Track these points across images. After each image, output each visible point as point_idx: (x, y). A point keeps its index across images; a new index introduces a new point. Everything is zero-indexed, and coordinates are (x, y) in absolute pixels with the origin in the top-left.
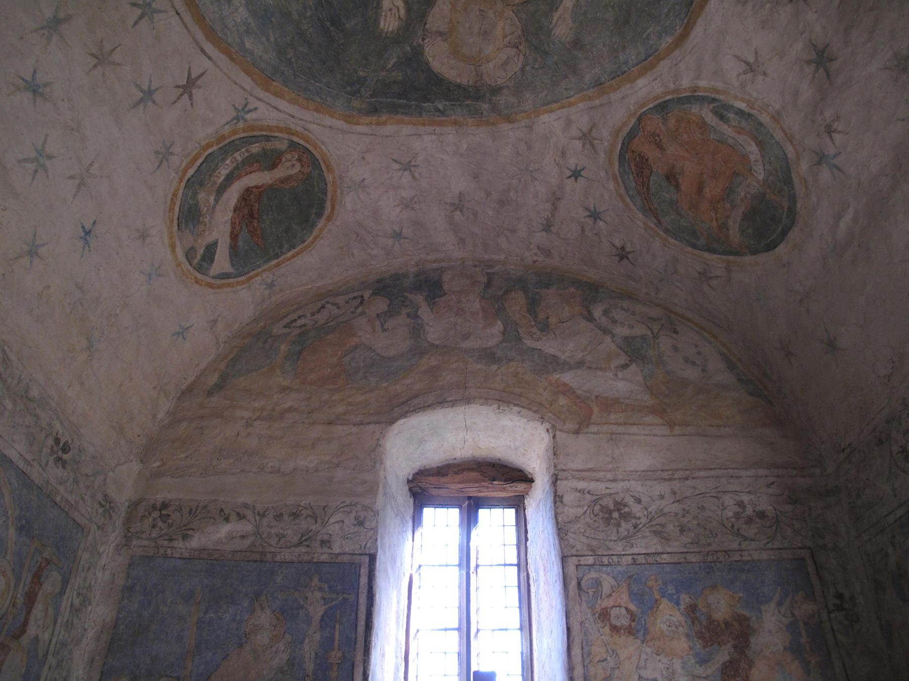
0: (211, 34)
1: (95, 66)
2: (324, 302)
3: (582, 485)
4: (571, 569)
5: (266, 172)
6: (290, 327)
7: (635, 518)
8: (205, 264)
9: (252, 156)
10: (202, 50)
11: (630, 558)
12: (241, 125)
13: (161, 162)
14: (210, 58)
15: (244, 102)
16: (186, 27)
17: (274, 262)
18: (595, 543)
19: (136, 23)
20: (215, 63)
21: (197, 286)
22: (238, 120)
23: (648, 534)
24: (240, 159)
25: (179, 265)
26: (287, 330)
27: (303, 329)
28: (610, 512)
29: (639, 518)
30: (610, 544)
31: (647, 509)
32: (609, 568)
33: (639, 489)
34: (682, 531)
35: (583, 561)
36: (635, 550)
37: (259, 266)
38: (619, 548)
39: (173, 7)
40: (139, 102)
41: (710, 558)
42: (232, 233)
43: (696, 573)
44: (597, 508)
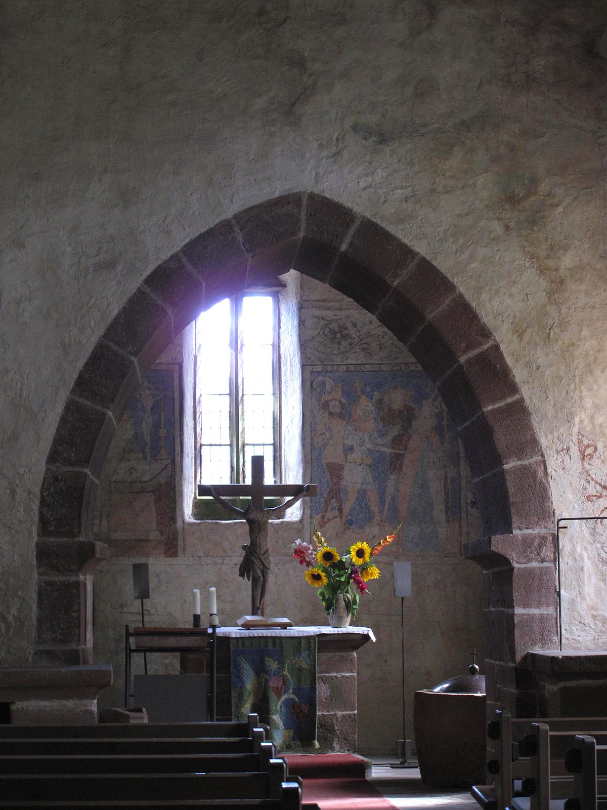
3: (318, 312)
4: (308, 374)
7: (351, 338)
11: (345, 367)
18: (323, 356)
23: (358, 350)
28: (335, 333)
29: (354, 338)
30: (333, 357)
31: (359, 332)
32: (331, 374)
33: (356, 316)
34: (380, 348)
35: (315, 369)
36: (349, 362)
38: (338, 360)
41: (396, 368)
43: (386, 378)
44: (327, 330)
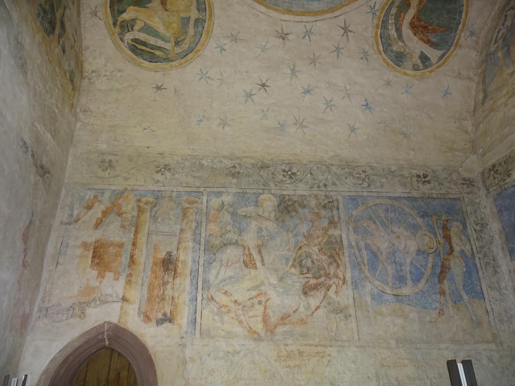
0: (332, 10)
1: (315, 65)
2: (504, 13)
5: (409, 10)
6: (497, 42)
8: (426, 64)
9: (396, 14)
10: (336, 17)
12: (378, 13)
13: (366, 59)
14: (341, 15)
15: (369, 7)
16: (324, 20)
17: (460, 26)
19: (310, 41)
20: (344, 14)
21: (433, 73)
22: (375, 13)
24: (393, 21)
25: (415, 76)
26: (496, 45)
27: (503, 36)
37: (455, 36)
39: (312, 22)
40: (338, 55)
42: (425, 42)
